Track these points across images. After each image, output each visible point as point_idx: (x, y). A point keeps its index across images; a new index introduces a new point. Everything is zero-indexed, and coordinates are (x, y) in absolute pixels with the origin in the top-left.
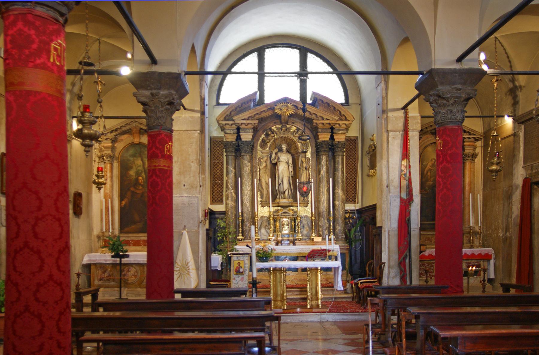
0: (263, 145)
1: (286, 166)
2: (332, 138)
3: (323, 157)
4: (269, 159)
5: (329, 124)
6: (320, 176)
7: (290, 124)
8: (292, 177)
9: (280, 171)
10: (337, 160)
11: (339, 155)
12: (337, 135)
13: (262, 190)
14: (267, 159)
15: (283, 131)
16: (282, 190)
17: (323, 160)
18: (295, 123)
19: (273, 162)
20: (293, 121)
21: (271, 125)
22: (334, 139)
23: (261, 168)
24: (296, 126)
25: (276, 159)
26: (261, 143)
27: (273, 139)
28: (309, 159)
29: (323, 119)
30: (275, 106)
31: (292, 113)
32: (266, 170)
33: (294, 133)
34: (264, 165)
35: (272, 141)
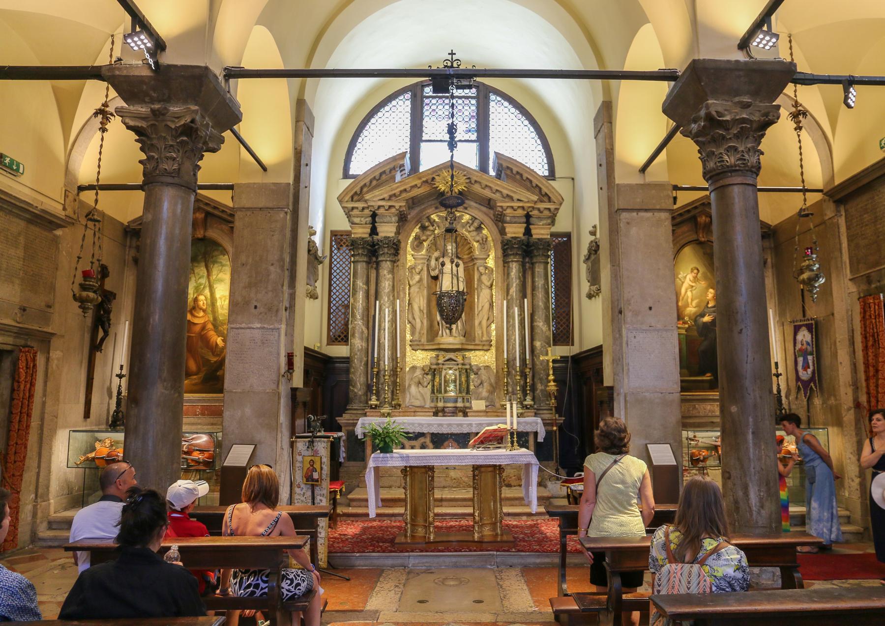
0: (417, 246)
2: (528, 232)
4: (425, 269)
12: (536, 228)
13: (413, 322)
19: (433, 274)
23: (411, 283)
25: (437, 270)
26: (413, 242)
27: (433, 236)
29: (511, 198)
34: (417, 278)
35: (431, 238)
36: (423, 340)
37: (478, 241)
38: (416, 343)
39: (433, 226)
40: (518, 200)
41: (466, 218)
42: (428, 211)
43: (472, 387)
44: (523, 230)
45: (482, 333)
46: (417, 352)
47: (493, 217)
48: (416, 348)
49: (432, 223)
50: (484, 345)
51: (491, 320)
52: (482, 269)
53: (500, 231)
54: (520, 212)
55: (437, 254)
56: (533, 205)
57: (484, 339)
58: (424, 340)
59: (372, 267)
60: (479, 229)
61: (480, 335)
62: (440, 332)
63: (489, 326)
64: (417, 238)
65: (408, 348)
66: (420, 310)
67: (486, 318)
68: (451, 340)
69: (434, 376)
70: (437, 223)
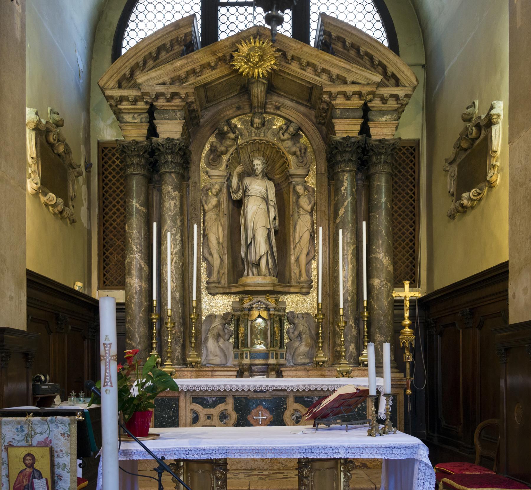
0: (214, 160)
1: (263, 206)
2: (365, 130)
3: (343, 176)
4: (225, 190)
5: (360, 95)
7: (272, 111)
8: (276, 232)
9: (249, 216)
10: (376, 183)
11: (381, 173)
13: (210, 258)
14: (220, 191)
15: (256, 128)
16: (253, 258)
17: (345, 184)
18: (282, 109)
19: (235, 197)
20: (277, 104)
21: (230, 113)
23: (206, 208)
24: (283, 114)
25: (241, 192)
26: (208, 155)
27: (235, 147)
28: (313, 190)
29: (344, 81)
30: (234, 51)
31: (272, 69)
32: (218, 215)
33: (279, 132)
34: (214, 201)
35: (231, 150)
36: (223, 282)
37: (294, 154)
38: (213, 285)
39: (234, 133)
40: (353, 83)
41: (279, 123)
42: (228, 113)
43: (286, 341)
44: (358, 128)
45: (300, 272)
46: (216, 297)
47: (314, 120)
48: (212, 291)
49: (233, 129)
50: (302, 287)
51: (311, 255)
52: (300, 189)
53: (324, 139)
54: (356, 102)
55: (239, 169)
56: (374, 89)
58: (224, 281)
59: (154, 187)
60: (295, 137)
61: (298, 274)
62: (246, 272)
63: (308, 263)
64: (213, 150)
65: (204, 293)
66: (219, 243)
67: (305, 252)
68: (259, 280)
69: (237, 326)
70: (239, 129)
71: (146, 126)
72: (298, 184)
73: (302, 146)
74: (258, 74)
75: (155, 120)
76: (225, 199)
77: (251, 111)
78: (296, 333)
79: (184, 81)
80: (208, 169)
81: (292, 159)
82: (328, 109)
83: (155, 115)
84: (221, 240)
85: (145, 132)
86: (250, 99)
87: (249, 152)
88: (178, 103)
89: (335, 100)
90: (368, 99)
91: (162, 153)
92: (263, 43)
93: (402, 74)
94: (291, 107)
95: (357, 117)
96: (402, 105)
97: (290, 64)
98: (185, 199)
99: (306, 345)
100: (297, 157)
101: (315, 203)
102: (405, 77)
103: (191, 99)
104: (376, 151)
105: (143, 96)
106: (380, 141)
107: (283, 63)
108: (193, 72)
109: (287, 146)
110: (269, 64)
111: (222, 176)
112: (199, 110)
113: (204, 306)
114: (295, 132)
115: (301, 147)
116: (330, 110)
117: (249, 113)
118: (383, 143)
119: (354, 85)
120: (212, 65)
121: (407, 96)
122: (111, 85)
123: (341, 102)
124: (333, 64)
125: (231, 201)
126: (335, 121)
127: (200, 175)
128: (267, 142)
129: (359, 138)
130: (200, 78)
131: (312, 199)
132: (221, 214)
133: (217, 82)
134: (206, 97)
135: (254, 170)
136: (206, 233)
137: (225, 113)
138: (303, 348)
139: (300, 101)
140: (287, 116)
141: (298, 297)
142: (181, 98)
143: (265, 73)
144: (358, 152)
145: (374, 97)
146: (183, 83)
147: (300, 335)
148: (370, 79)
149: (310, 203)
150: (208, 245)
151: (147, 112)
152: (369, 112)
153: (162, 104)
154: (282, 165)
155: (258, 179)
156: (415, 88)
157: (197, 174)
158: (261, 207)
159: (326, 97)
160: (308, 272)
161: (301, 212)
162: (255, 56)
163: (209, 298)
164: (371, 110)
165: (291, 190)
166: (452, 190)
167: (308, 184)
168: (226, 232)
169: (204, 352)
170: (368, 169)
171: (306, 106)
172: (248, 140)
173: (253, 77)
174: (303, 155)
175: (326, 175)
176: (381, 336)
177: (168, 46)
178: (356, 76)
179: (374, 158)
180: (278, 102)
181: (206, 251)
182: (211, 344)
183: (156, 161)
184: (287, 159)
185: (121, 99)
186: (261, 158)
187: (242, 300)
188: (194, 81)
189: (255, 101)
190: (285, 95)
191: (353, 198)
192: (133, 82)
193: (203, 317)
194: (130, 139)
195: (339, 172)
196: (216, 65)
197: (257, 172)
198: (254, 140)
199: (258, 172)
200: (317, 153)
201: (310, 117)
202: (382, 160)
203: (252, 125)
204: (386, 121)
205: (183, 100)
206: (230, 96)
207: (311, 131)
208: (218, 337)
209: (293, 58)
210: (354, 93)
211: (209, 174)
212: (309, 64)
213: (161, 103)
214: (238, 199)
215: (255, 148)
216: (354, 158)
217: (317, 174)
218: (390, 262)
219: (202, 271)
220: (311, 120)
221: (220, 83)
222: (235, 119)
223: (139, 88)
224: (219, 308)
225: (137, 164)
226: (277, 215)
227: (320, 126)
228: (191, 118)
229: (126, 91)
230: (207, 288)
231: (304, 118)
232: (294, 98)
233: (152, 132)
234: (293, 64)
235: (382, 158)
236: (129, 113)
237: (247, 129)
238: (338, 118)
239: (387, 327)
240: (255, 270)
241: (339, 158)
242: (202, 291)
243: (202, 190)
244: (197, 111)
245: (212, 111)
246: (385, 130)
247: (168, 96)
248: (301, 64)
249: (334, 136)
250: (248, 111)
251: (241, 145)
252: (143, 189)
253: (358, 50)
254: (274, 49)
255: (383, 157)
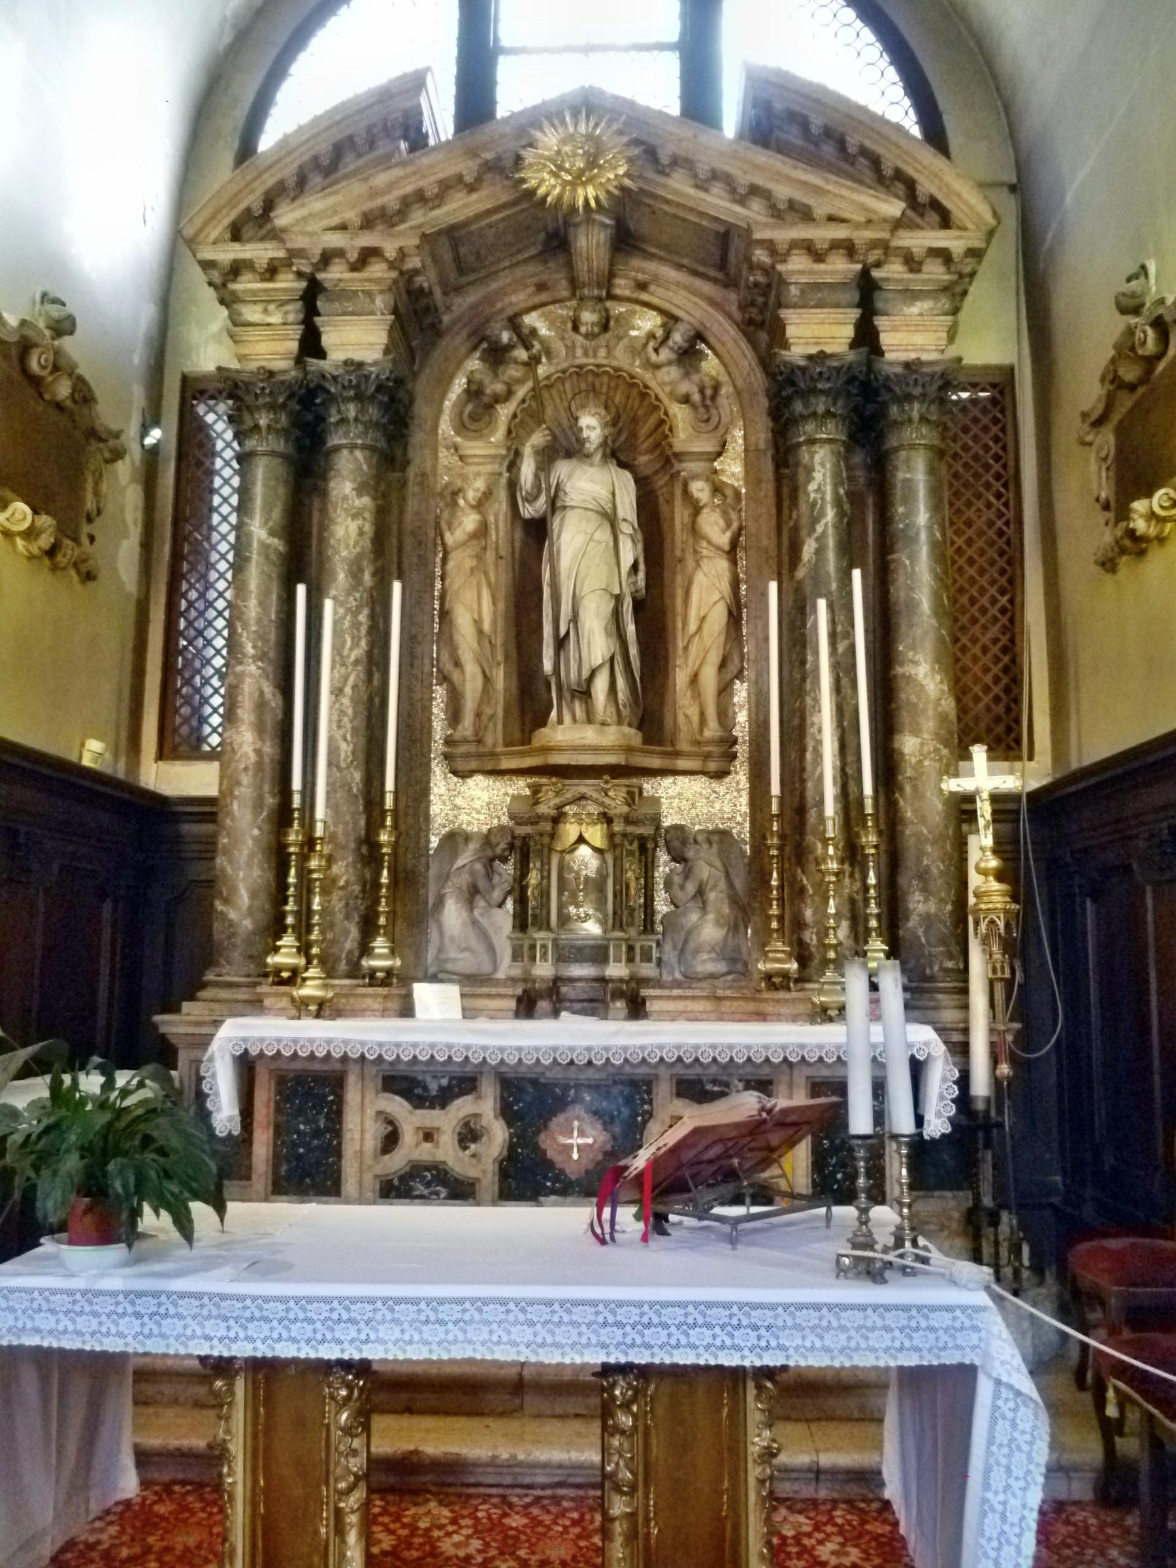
1: (605, 535)
4: (502, 494)
5: (849, 249)
6: (801, 573)
7: (627, 293)
8: (638, 606)
9: (565, 562)
10: (901, 475)
11: (913, 447)
12: (895, 329)
13: (456, 676)
14: (488, 495)
15: (587, 336)
16: (573, 675)
17: (818, 476)
18: (652, 288)
19: (528, 511)
20: (640, 276)
22: (876, 350)
23: (449, 539)
24: (655, 301)
25: (543, 499)
27: (530, 384)
28: (737, 494)
29: (806, 215)
30: (524, 147)
31: (622, 188)
32: (479, 557)
33: (645, 345)
34: (469, 522)
35: (521, 392)
36: (489, 740)
37: (686, 400)
39: (528, 347)
40: (831, 219)
41: (647, 323)
42: (514, 299)
43: (662, 906)
44: (848, 332)
45: (702, 714)
46: (470, 782)
47: (738, 316)
49: (526, 338)
50: (707, 757)
51: (733, 668)
52: (700, 490)
54: (840, 267)
55: (538, 438)
56: (885, 235)
57: (708, 734)
58: (494, 737)
60: (688, 356)
61: (695, 719)
62: (554, 714)
63: (725, 690)
64: (474, 392)
65: (438, 770)
66: (480, 632)
67: (714, 659)
68: (589, 735)
70: (542, 342)
71: (296, 332)
72: (695, 477)
73: (706, 379)
74: (586, 200)
75: (319, 314)
76: (501, 518)
77: (574, 295)
78: (691, 888)
79: (395, 219)
80: (458, 439)
81: (680, 414)
82: (769, 285)
83: (319, 304)
84: (487, 626)
85: (294, 346)
86: (569, 265)
87: (570, 396)
88: (380, 275)
89: (785, 261)
90: (872, 257)
91: (331, 399)
92: (596, 125)
93: (955, 199)
94: (678, 284)
95: (843, 303)
96: (961, 276)
97: (667, 175)
98: (394, 517)
99: (718, 923)
100: (694, 407)
101: (740, 529)
102: (963, 207)
103: (414, 262)
104: (897, 389)
105: (290, 258)
106: (907, 365)
107: (650, 175)
108: (420, 197)
109: (667, 379)
110: (611, 176)
111: (494, 457)
112: (438, 292)
113: (438, 808)
114: (686, 345)
115: (702, 382)
116: (774, 286)
117: (569, 299)
118: (916, 372)
119: (834, 224)
120: (469, 179)
121: (975, 254)
122: (214, 235)
123: (801, 267)
124: (778, 173)
125: (519, 524)
126: (786, 314)
127: (436, 458)
128: (616, 370)
129: (851, 357)
130: (436, 212)
131: (734, 516)
132: (490, 556)
133: (483, 223)
134: (458, 260)
135: (581, 442)
136: (447, 606)
137: (507, 300)
138: (710, 932)
139: (701, 269)
140: (667, 306)
141: (698, 785)
142: (387, 260)
143: (603, 196)
144: (849, 394)
145: (886, 254)
146: (393, 226)
147: (700, 893)
148: (874, 212)
149: (728, 526)
150: (451, 637)
151: (302, 298)
152: (876, 294)
153: (338, 276)
154: (656, 430)
155: (592, 465)
156: (991, 233)
157: (427, 452)
158: (597, 536)
159: (761, 256)
160: (725, 716)
161: (705, 552)
162: (575, 155)
163: (452, 786)
164: (880, 288)
165: (678, 492)
166: (1103, 495)
167: (724, 479)
168: (501, 605)
169: (434, 935)
170: (881, 437)
171: (715, 281)
172: (564, 365)
173: (573, 209)
174: (708, 402)
175: (769, 454)
176: (926, 900)
177: (359, 140)
178: (837, 203)
179: (894, 410)
180: (644, 272)
181: (445, 656)
182: (453, 915)
183: (321, 419)
184: (666, 414)
185: (236, 269)
186: (603, 412)
187: (536, 790)
188: (422, 220)
189: (582, 267)
190: (662, 253)
191: (841, 514)
192: (269, 226)
193: (433, 838)
194: (253, 366)
195: (800, 445)
196: (479, 180)
197: (587, 445)
198: (581, 367)
199: (590, 447)
200: (746, 395)
201: (727, 308)
202: (915, 415)
203: (576, 328)
204: (921, 315)
205: (392, 265)
206: (520, 257)
207: (730, 344)
208: (472, 894)
209: (675, 162)
210: (835, 245)
211: (461, 452)
212: (715, 176)
213: (335, 274)
214: (536, 516)
215: (583, 386)
216: (839, 408)
217: (746, 450)
218: (946, 688)
219: (435, 711)
220: (728, 315)
221: (490, 226)
222: (534, 314)
223: (282, 241)
224: (478, 813)
225: (269, 427)
226: (641, 560)
227: (752, 329)
228: (415, 311)
229: (249, 246)
230: (447, 757)
231: (711, 310)
232: (685, 261)
233: (311, 345)
234: (675, 175)
235: (916, 410)
236: (255, 302)
237: (563, 339)
238: (795, 306)
239: (942, 874)
240: (578, 708)
241: (798, 407)
242: (433, 764)
243: (441, 495)
244: (431, 293)
245: (473, 296)
246: (920, 339)
247: (353, 256)
248: (695, 176)
249: (784, 352)
250: (566, 293)
251: (548, 378)
252: (282, 491)
253: (841, 144)
254: (625, 139)
255: (916, 406)
